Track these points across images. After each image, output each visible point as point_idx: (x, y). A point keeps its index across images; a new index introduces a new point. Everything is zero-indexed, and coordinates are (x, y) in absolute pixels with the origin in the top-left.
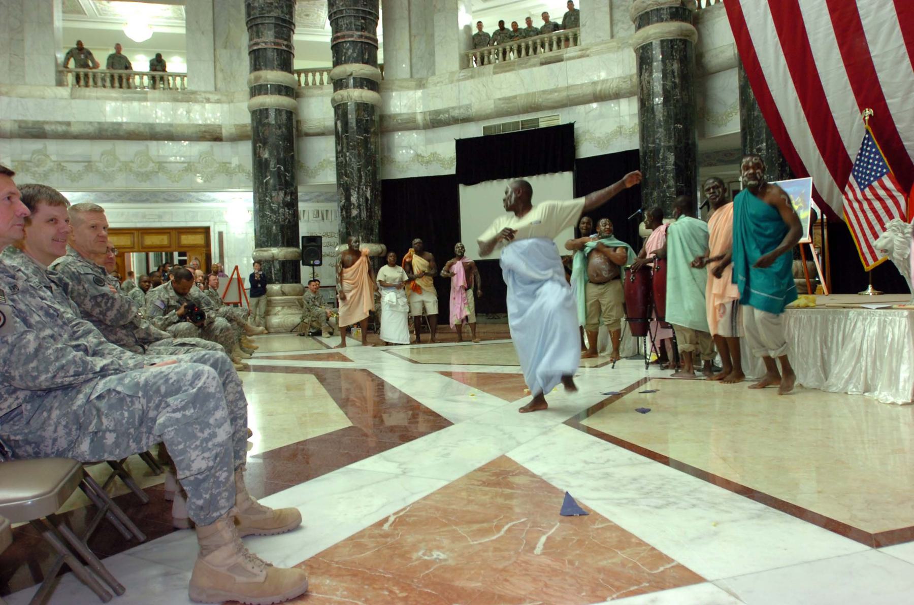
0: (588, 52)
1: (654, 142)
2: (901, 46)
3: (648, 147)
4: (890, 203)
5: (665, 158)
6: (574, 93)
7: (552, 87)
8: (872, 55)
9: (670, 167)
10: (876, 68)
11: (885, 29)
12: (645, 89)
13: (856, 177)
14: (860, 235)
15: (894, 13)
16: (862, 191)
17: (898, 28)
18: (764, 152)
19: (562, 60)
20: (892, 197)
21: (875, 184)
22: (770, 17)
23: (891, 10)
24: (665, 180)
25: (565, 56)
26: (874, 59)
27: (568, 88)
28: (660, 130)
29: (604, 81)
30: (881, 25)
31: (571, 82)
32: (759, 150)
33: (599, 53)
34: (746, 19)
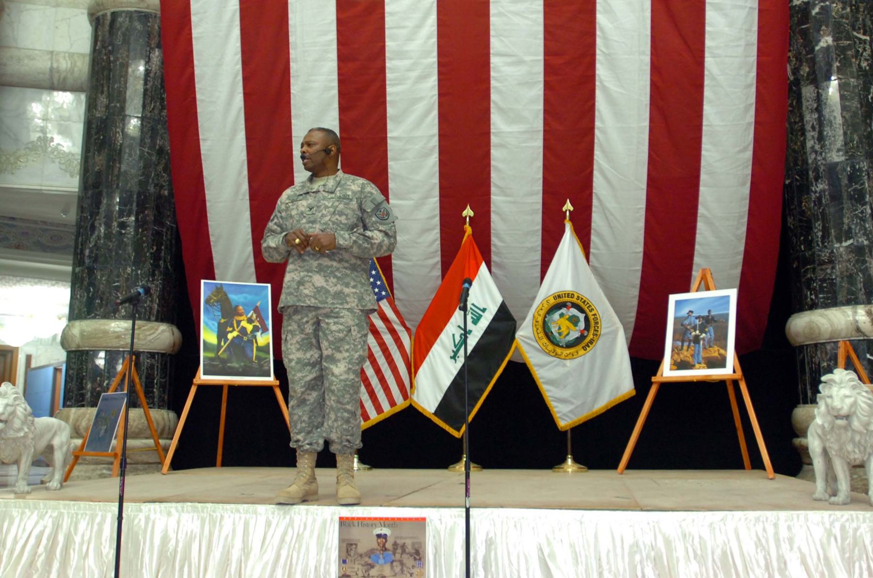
2: (433, 136)
4: (388, 338)
8: (389, 135)
10: (390, 155)
11: (420, 108)
15: (436, 92)
17: (435, 113)
18: (131, 230)
20: (393, 332)
22: (236, 32)
23: (433, 87)
26: (389, 141)
30: (416, 101)
32: (123, 225)
34: (194, 19)
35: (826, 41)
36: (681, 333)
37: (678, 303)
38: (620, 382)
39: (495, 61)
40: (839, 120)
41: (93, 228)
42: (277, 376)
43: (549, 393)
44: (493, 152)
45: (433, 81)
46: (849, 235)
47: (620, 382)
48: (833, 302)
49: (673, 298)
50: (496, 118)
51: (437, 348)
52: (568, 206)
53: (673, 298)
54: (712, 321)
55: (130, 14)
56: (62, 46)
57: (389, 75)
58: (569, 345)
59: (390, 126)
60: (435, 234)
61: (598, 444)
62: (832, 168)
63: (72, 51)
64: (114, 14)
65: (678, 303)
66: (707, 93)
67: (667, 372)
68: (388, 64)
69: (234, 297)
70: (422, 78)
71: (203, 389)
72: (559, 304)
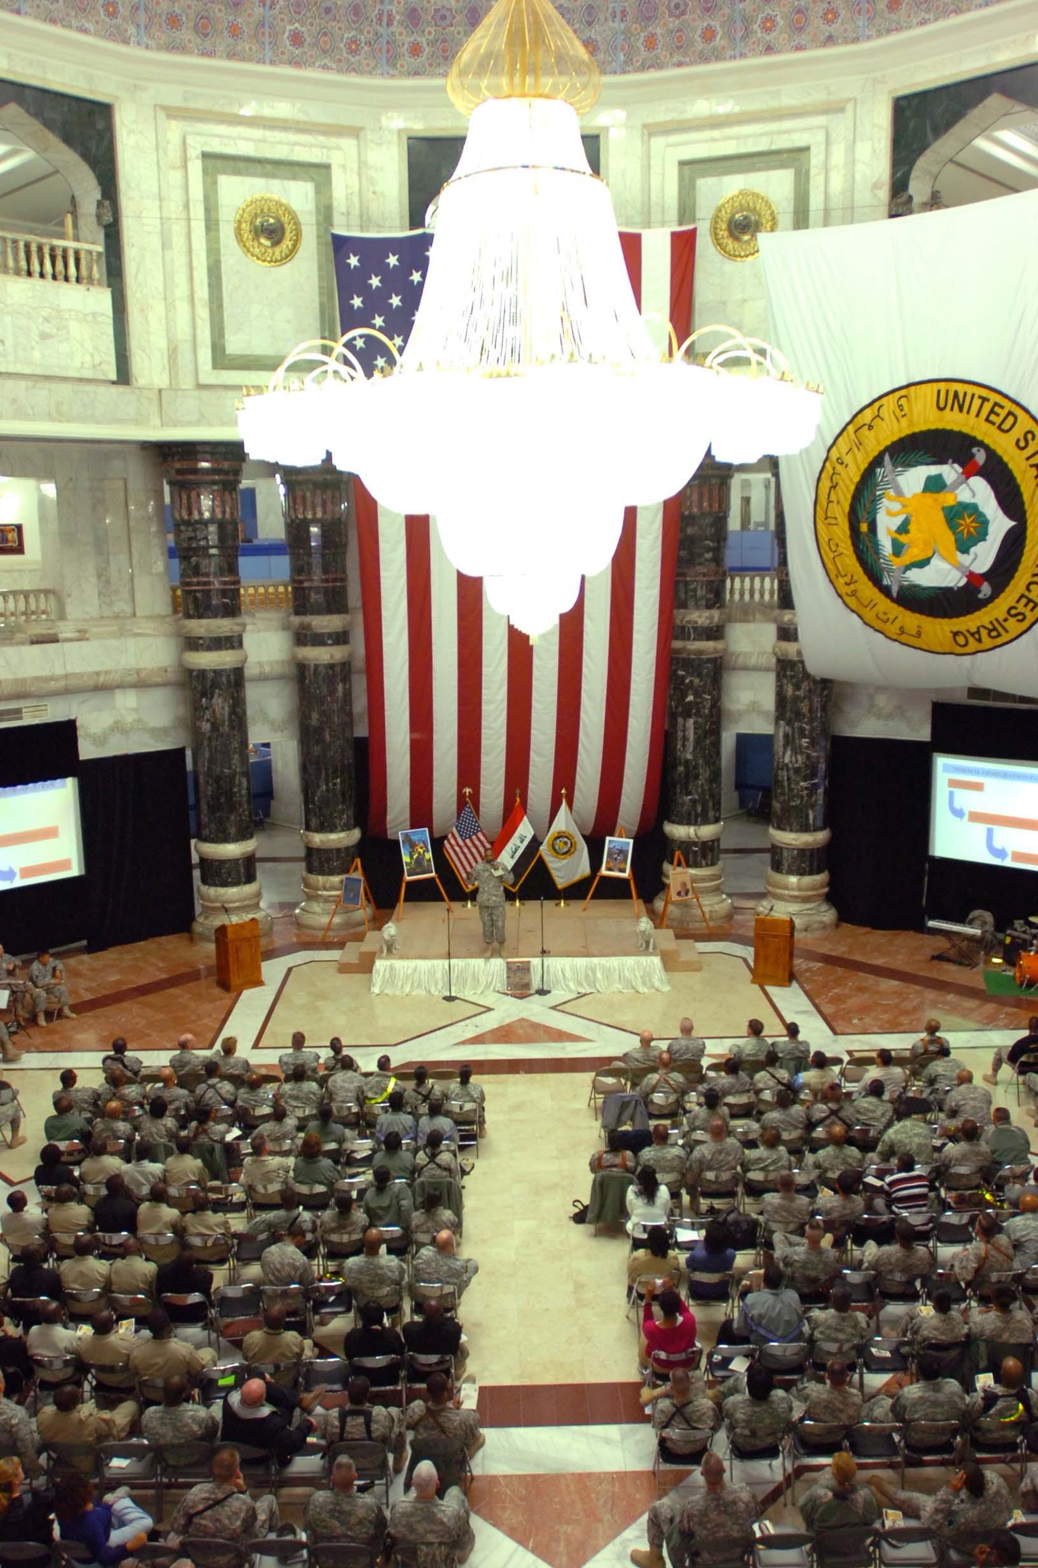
0: (87, 636)
1: (230, 768)
3: (222, 772)
5: (240, 784)
6: (74, 682)
7: (45, 673)
9: (244, 792)
12: (218, 715)
13: (459, 831)
14: (459, 865)
16: (464, 841)
19: (54, 639)
21: (474, 837)
24: (240, 806)
25: (61, 636)
27: (66, 676)
28: (236, 756)
29: (107, 673)
31: (70, 669)
32: (335, 784)
33: (99, 637)
35: (690, 698)
36: (610, 855)
37: (610, 842)
38: (583, 867)
39: (533, 732)
40: (692, 738)
41: (319, 787)
42: (437, 872)
43: (555, 874)
44: (531, 768)
45: (504, 739)
46: (690, 793)
47: (583, 867)
48: (680, 823)
49: (608, 839)
50: (532, 754)
51: (504, 852)
52: (563, 791)
53: (608, 839)
54: (622, 852)
55: (324, 665)
56: (265, 658)
57: (483, 736)
58: (564, 854)
59: (482, 756)
60: (501, 799)
61: (577, 891)
62: (687, 761)
63: (273, 659)
64: (316, 666)
65: (610, 842)
66: (628, 748)
67: (604, 872)
68: (483, 731)
69: (414, 838)
70: (499, 738)
71: (409, 884)
72: (559, 836)
